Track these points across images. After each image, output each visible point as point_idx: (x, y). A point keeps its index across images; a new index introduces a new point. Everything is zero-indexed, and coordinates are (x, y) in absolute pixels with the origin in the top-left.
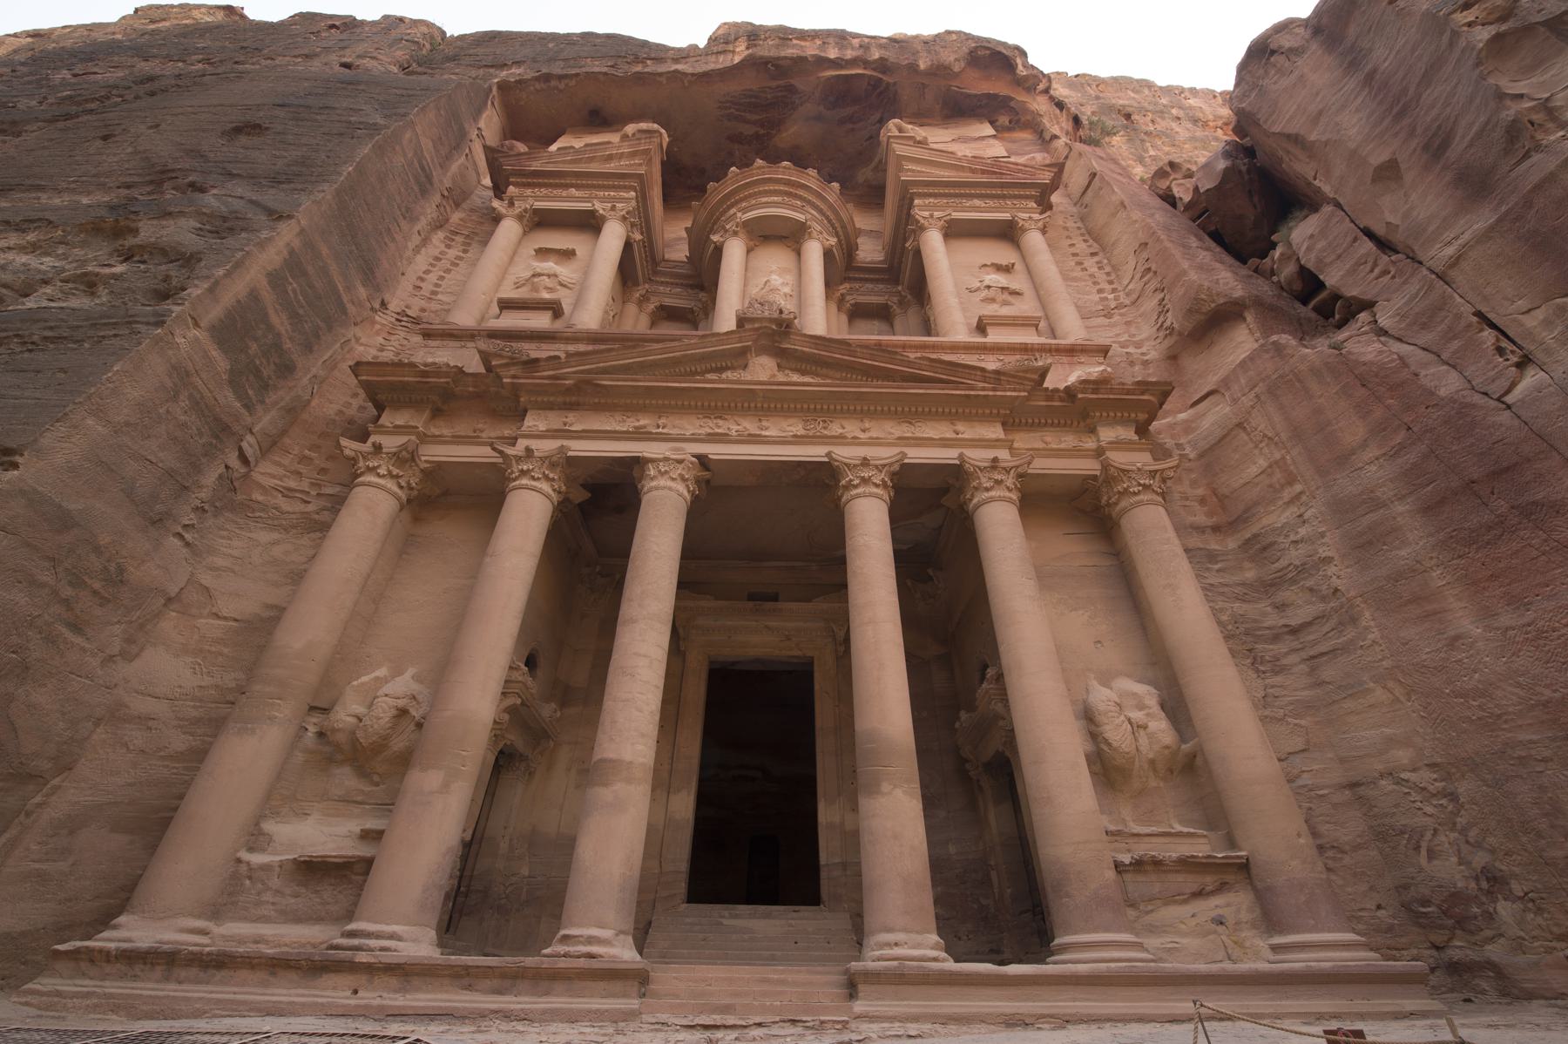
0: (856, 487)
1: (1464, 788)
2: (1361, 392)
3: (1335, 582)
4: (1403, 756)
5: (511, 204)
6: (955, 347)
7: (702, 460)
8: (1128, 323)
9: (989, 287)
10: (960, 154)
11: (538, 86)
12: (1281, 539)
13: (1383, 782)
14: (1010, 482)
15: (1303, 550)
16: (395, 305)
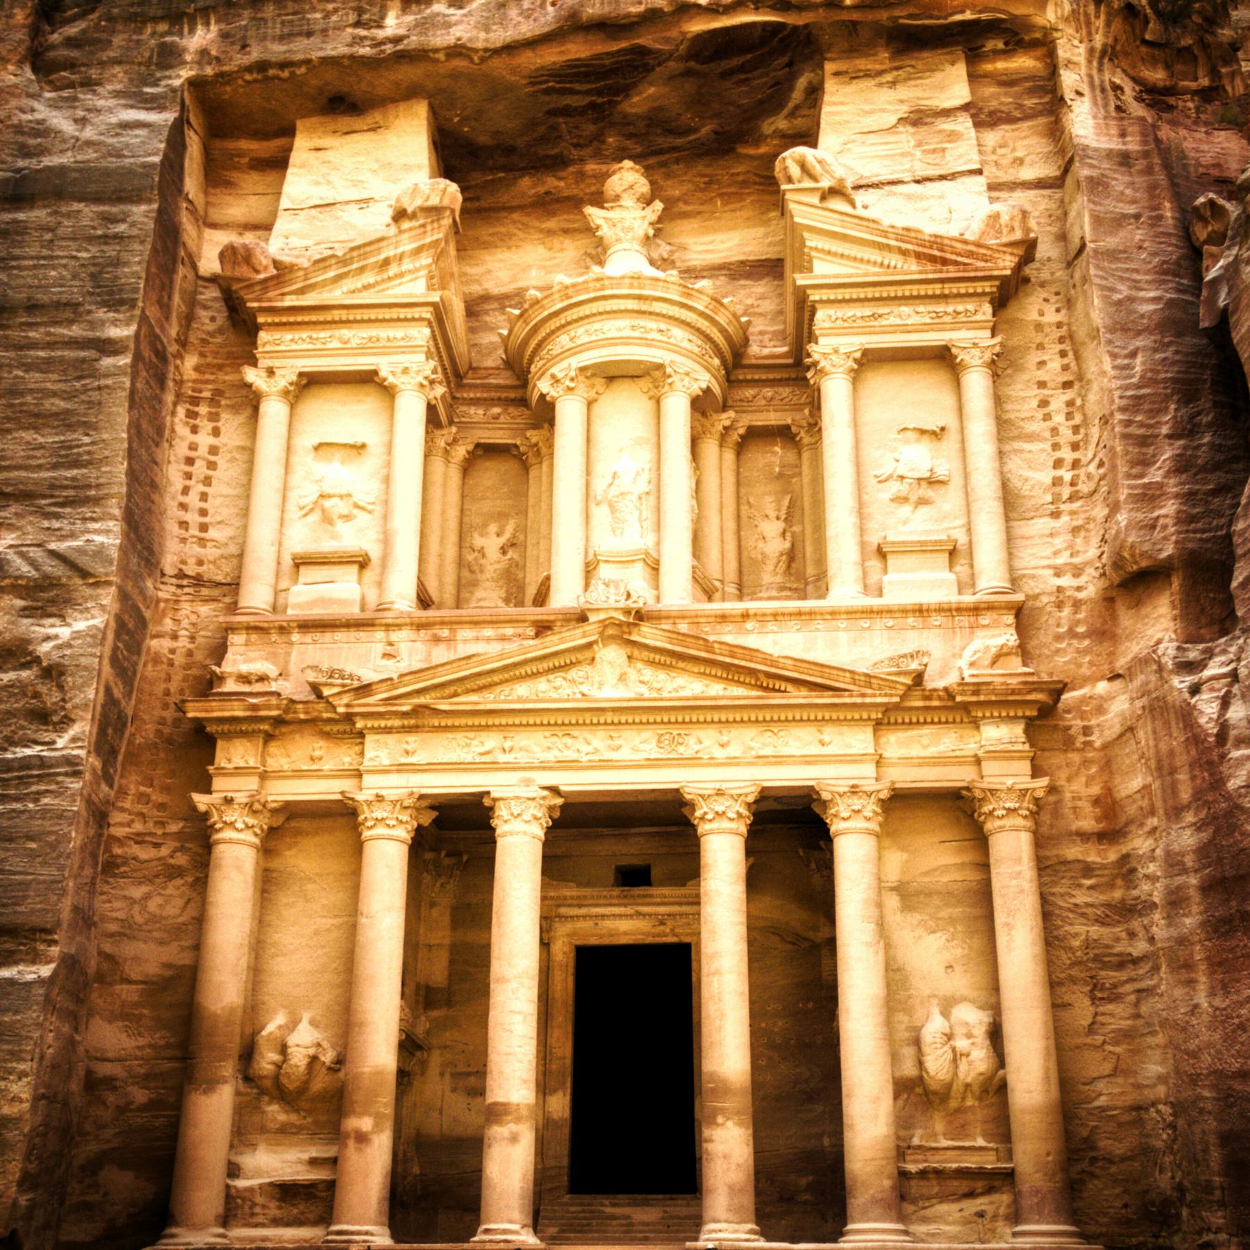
4: (1161, 1091)
5: (271, 372)
6: (834, 614)
7: (554, 790)
8: (1075, 530)
9: (902, 478)
10: (886, 222)
11: (248, 77)
14: (871, 807)
15: (1146, 887)
16: (169, 570)
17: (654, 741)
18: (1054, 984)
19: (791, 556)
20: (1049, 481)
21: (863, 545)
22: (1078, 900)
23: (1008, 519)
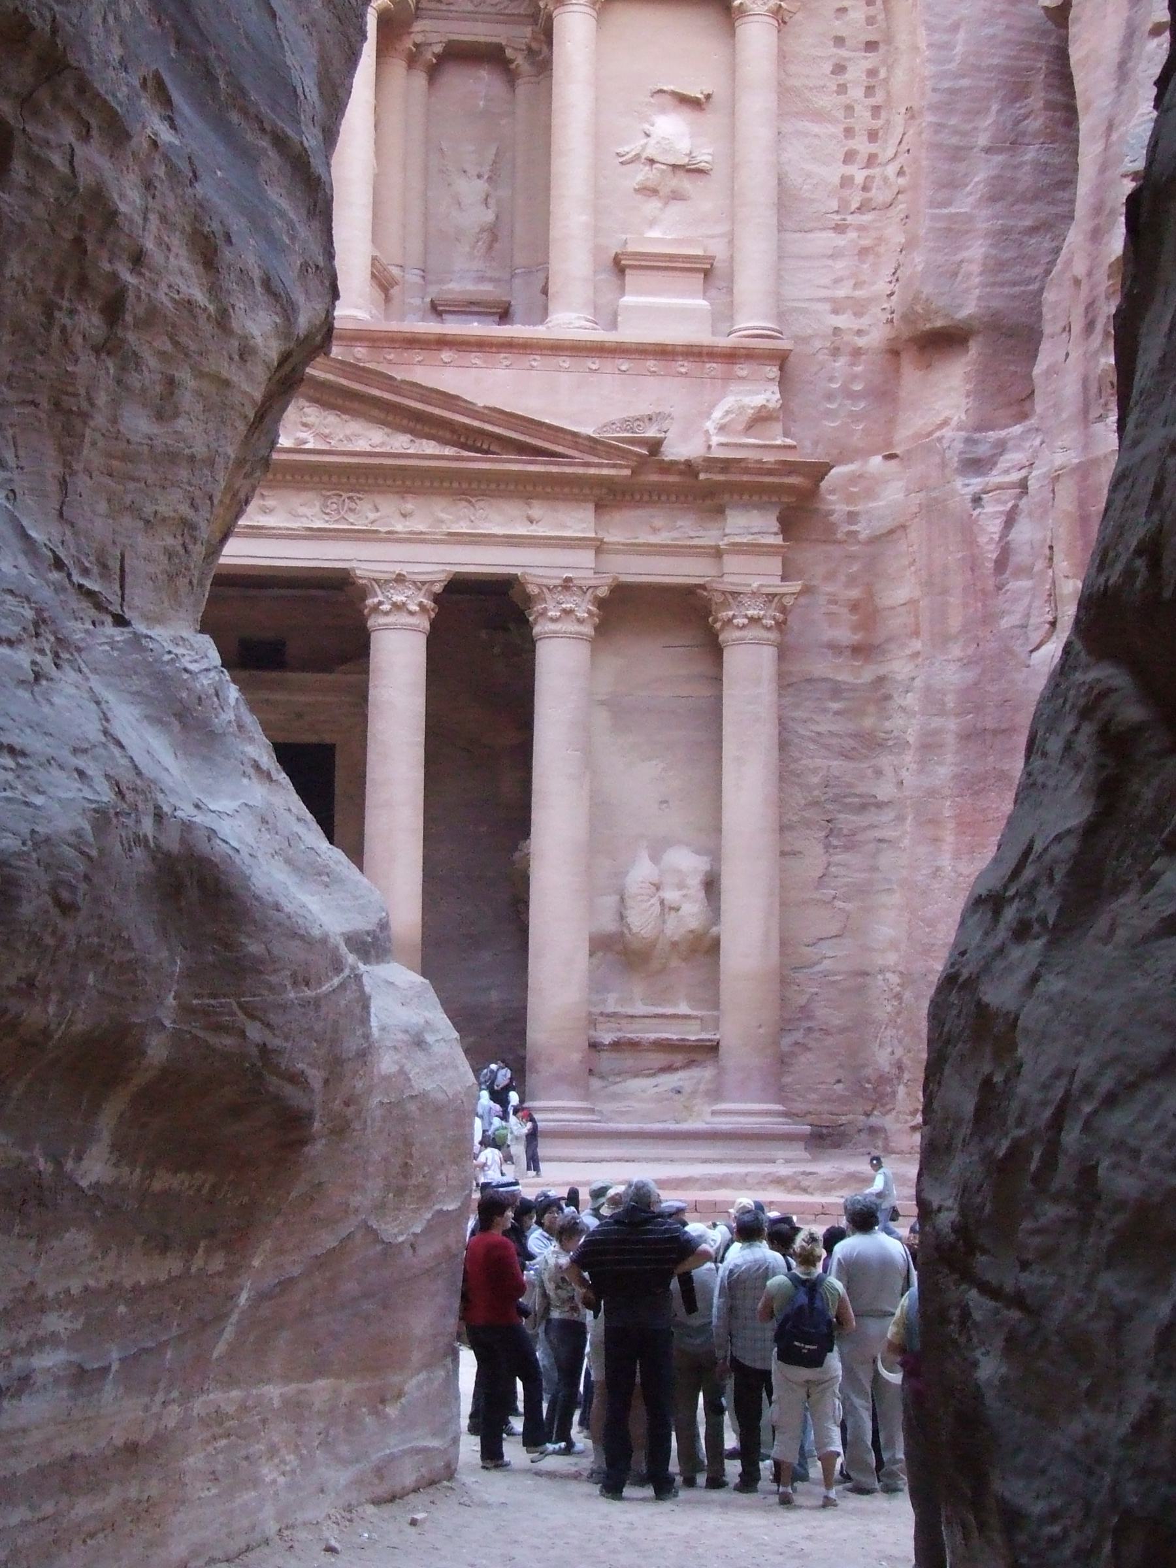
0: (387, 613)
1: (907, 995)
2: (969, 575)
3: (904, 774)
4: (892, 958)
6: (556, 348)
8: (863, 252)
9: (652, 161)
12: (895, 696)
13: (880, 977)
14: (583, 607)
17: (318, 504)
18: (783, 828)
19: (493, 234)
20: (836, 180)
21: (597, 250)
22: (819, 729)
23: (781, 228)
